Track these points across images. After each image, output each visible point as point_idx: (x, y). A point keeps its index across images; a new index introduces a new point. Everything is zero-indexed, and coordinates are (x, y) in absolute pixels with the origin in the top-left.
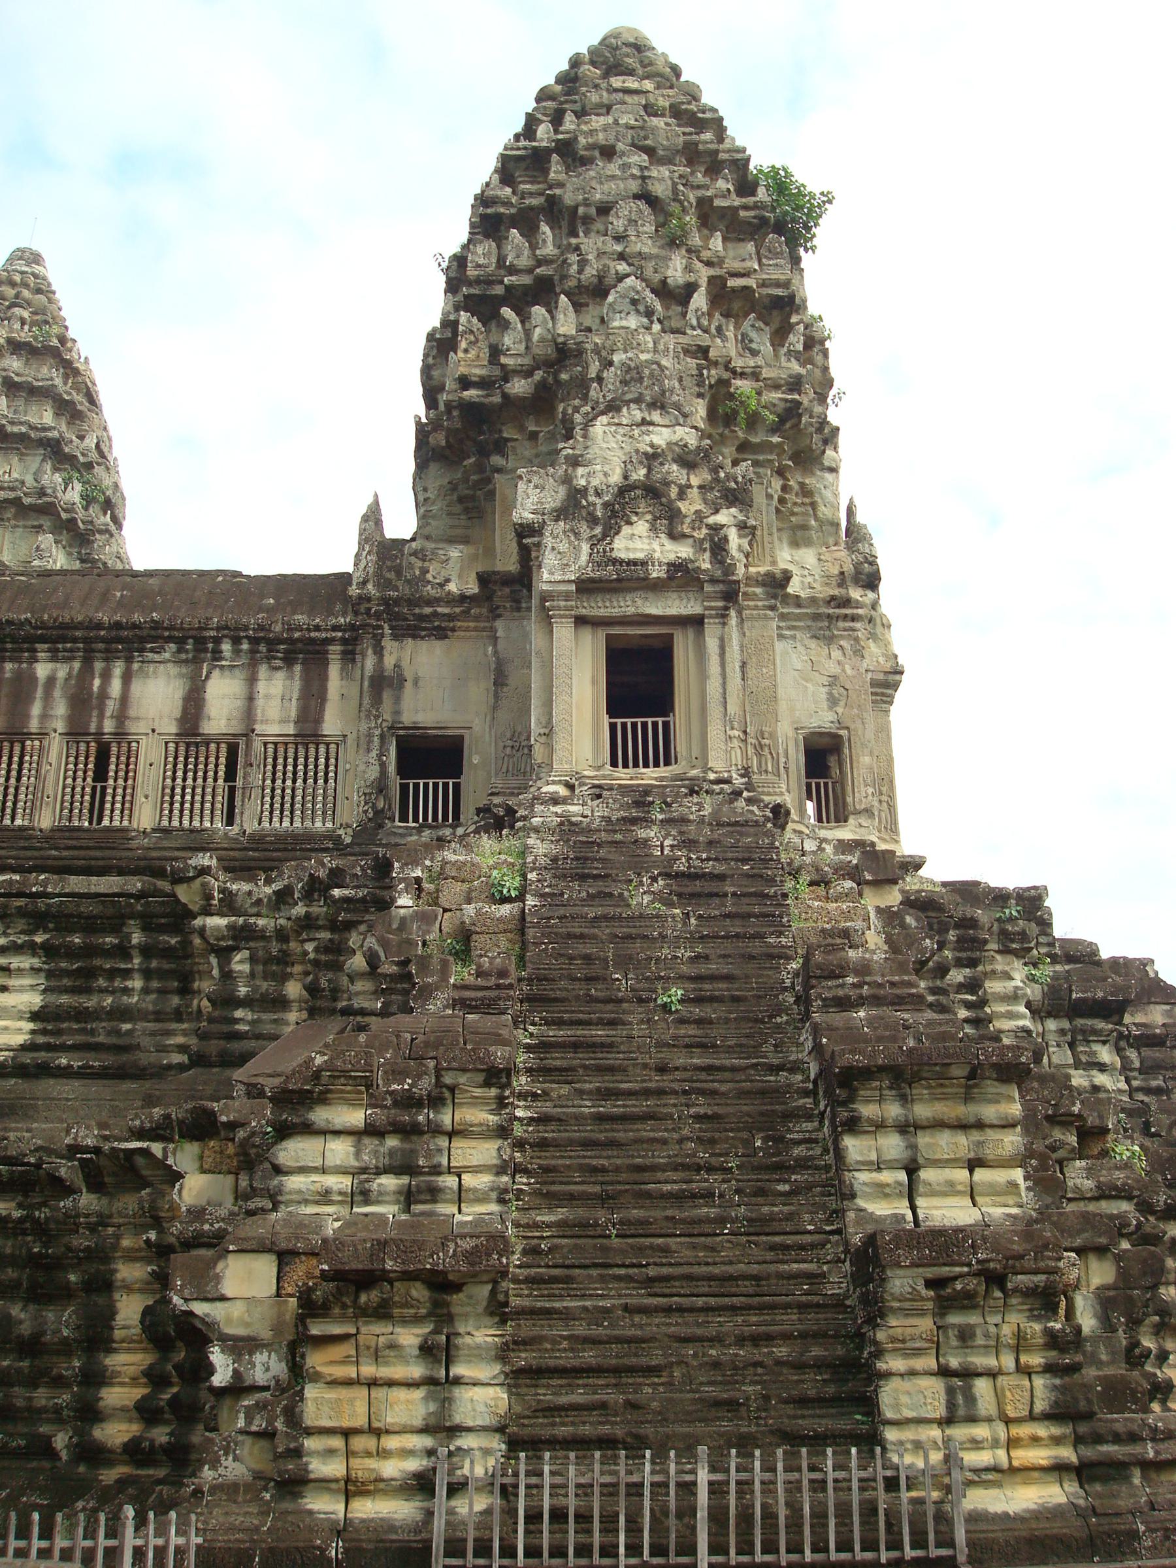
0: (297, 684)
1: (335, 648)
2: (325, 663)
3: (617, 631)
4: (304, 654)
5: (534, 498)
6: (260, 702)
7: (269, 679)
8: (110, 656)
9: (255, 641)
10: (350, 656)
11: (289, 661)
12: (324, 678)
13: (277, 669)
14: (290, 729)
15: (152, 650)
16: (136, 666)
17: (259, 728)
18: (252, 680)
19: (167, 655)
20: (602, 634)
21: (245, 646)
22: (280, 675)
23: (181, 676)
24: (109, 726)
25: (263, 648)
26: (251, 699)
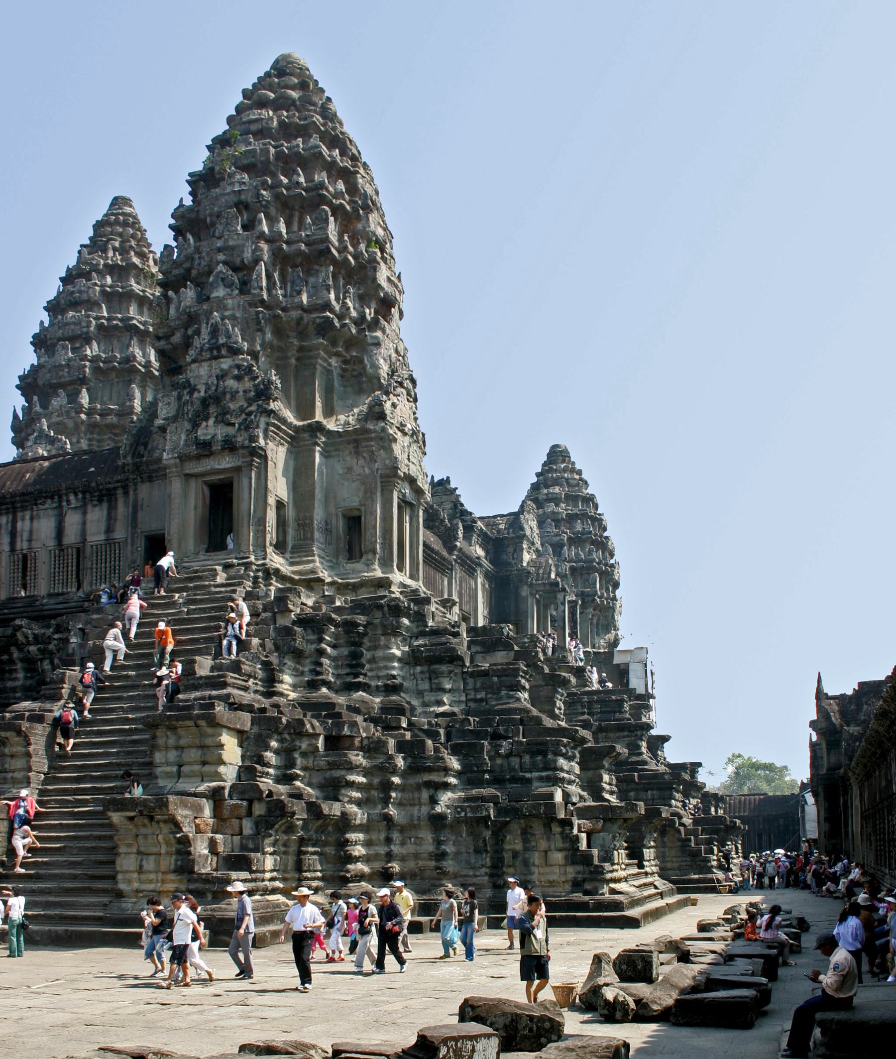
0: (105, 512)
1: (120, 492)
2: (116, 500)
3: (208, 478)
4: (106, 496)
5: (164, 412)
6: (88, 525)
7: (92, 512)
8: (24, 508)
9: (84, 493)
10: (126, 493)
11: (100, 501)
12: (116, 508)
13: (95, 506)
14: (102, 537)
15: (41, 504)
16: (35, 513)
17: (89, 539)
18: (85, 513)
19: (47, 506)
20: (200, 480)
21: (80, 496)
22: (97, 509)
23: (55, 515)
24: (25, 545)
25: (88, 496)
26: (84, 523)
